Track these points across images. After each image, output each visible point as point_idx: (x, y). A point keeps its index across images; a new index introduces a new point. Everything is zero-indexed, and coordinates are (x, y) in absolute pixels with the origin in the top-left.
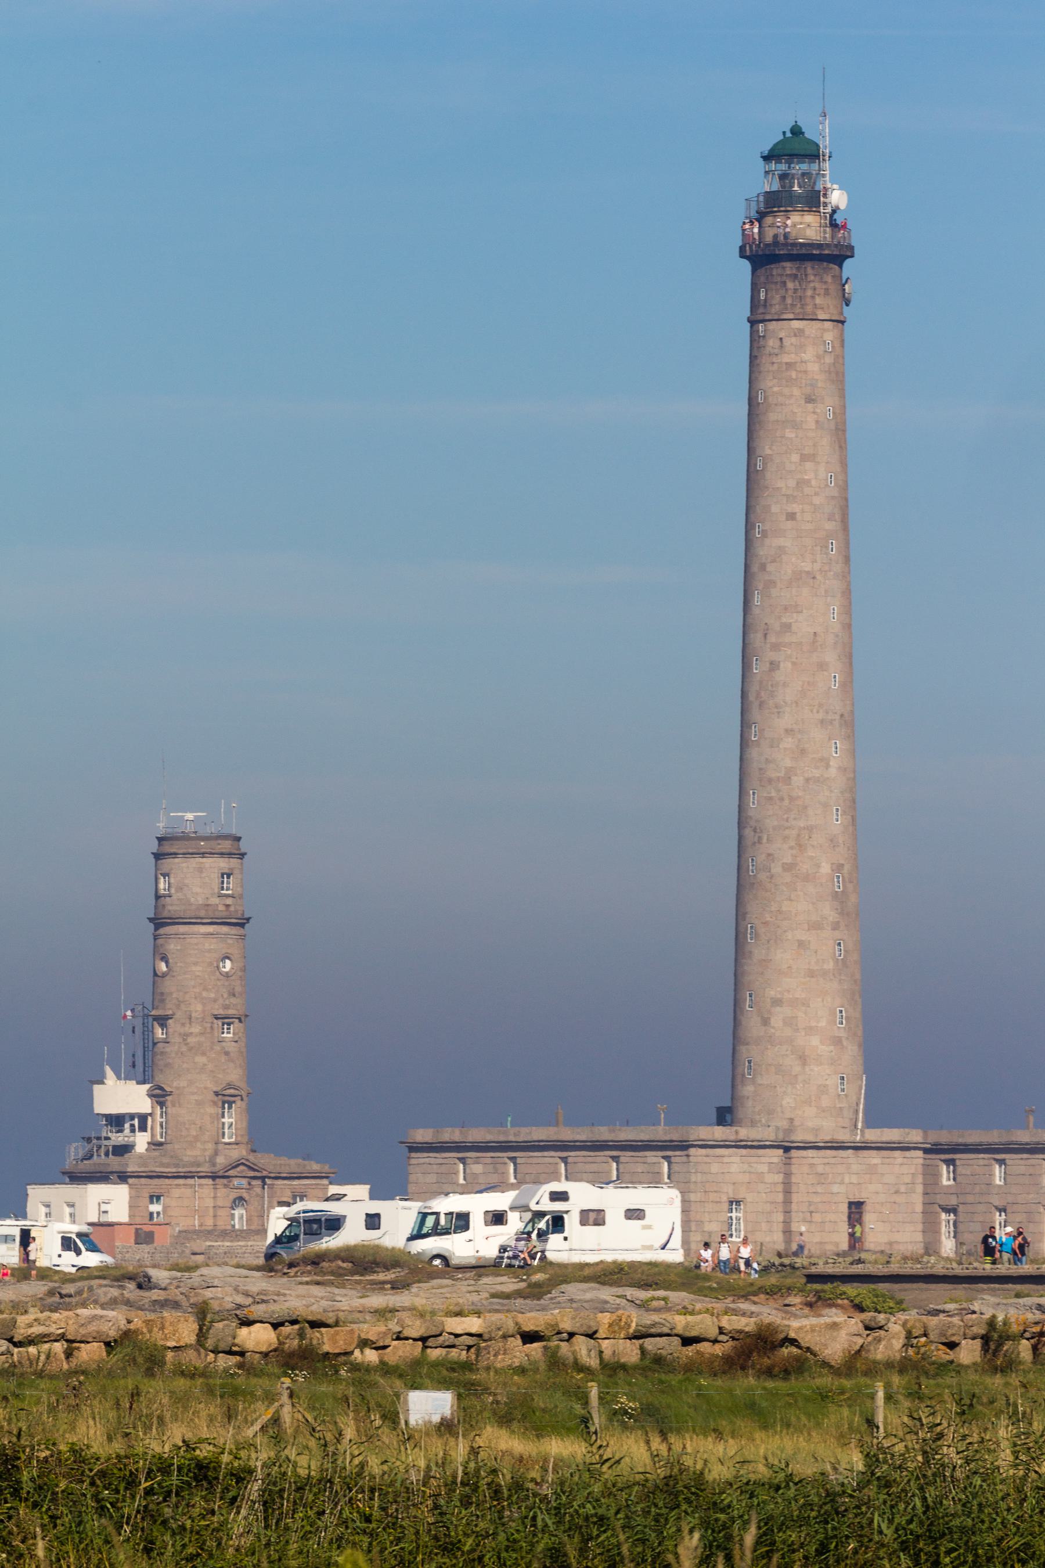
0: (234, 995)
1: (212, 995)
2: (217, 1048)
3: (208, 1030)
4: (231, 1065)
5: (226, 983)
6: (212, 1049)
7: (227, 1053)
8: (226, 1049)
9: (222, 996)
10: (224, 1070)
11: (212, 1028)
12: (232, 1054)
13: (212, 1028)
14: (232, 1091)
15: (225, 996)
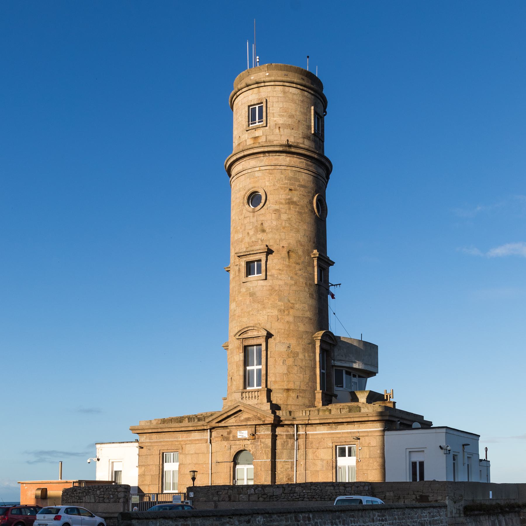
0: (263, 231)
1: (240, 236)
2: (243, 290)
3: (237, 274)
4: (256, 306)
5: (253, 220)
6: (240, 292)
7: (252, 295)
8: (252, 291)
9: (248, 233)
10: (249, 312)
11: (239, 270)
12: (259, 294)
13: (239, 270)
14: (255, 334)
15: (251, 233)
